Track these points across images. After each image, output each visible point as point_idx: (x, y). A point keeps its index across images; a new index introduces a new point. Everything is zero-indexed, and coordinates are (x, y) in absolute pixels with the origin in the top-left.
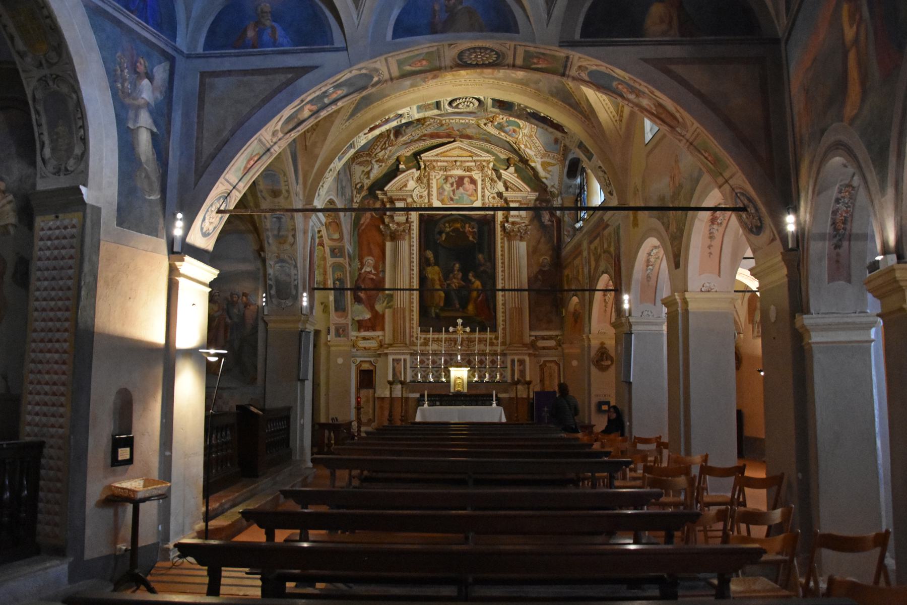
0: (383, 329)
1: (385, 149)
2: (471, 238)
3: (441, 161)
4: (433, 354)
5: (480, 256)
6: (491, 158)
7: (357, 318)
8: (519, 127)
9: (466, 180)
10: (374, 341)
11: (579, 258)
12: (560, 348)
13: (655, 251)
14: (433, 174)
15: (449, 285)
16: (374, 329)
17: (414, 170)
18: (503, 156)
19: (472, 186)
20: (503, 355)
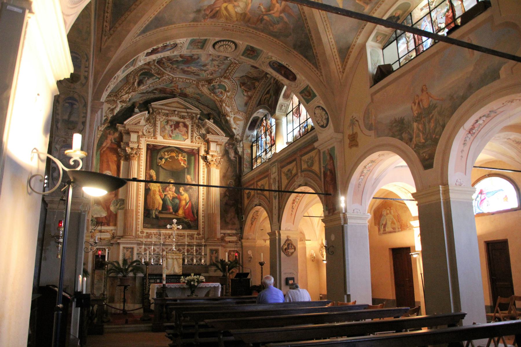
0: (115, 225)
1: (129, 93)
2: (182, 164)
3: (164, 110)
4: (145, 245)
5: (188, 177)
6: (198, 112)
7: (95, 216)
8: (225, 90)
9: (181, 124)
10: (108, 234)
11: (267, 178)
12: (240, 242)
13: (370, 164)
14: (158, 117)
15: (165, 195)
16: (108, 225)
17: (147, 112)
18: (205, 112)
19: (185, 129)
20: (205, 246)
